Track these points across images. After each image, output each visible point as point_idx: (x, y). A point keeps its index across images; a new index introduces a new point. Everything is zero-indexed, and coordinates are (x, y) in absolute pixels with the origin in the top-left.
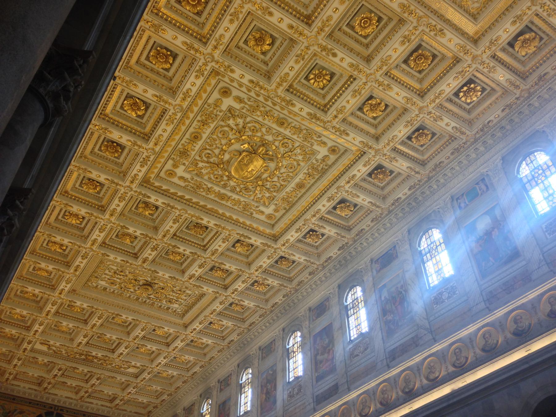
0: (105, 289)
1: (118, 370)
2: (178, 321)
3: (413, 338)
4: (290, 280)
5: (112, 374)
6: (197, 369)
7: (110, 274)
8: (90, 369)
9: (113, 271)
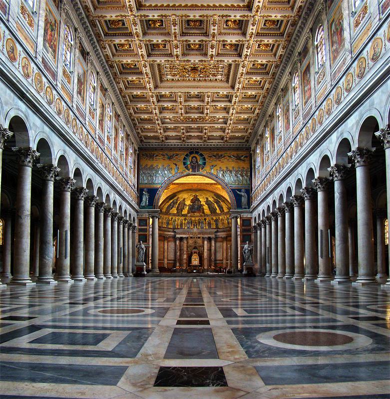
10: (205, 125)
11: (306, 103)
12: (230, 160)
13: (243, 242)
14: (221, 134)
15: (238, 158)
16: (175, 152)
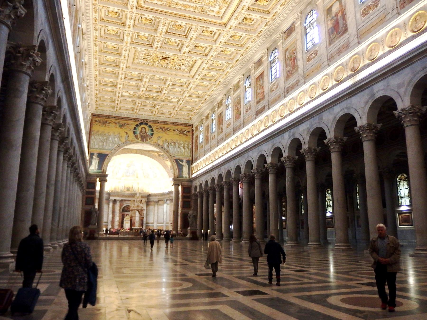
0: (144, 63)
1: (167, 101)
2: (188, 75)
3: (296, 81)
4: (242, 46)
5: (165, 103)
6: (206, 97)
7: (143, 56)
8: (153, 102)
9: (144, 54)
10: (159, 102)
11: (258, 102)
12: (175, 133)
13: (183, 207)
14: (172, 111)
15: (182, 132)
16: (126, 122)
